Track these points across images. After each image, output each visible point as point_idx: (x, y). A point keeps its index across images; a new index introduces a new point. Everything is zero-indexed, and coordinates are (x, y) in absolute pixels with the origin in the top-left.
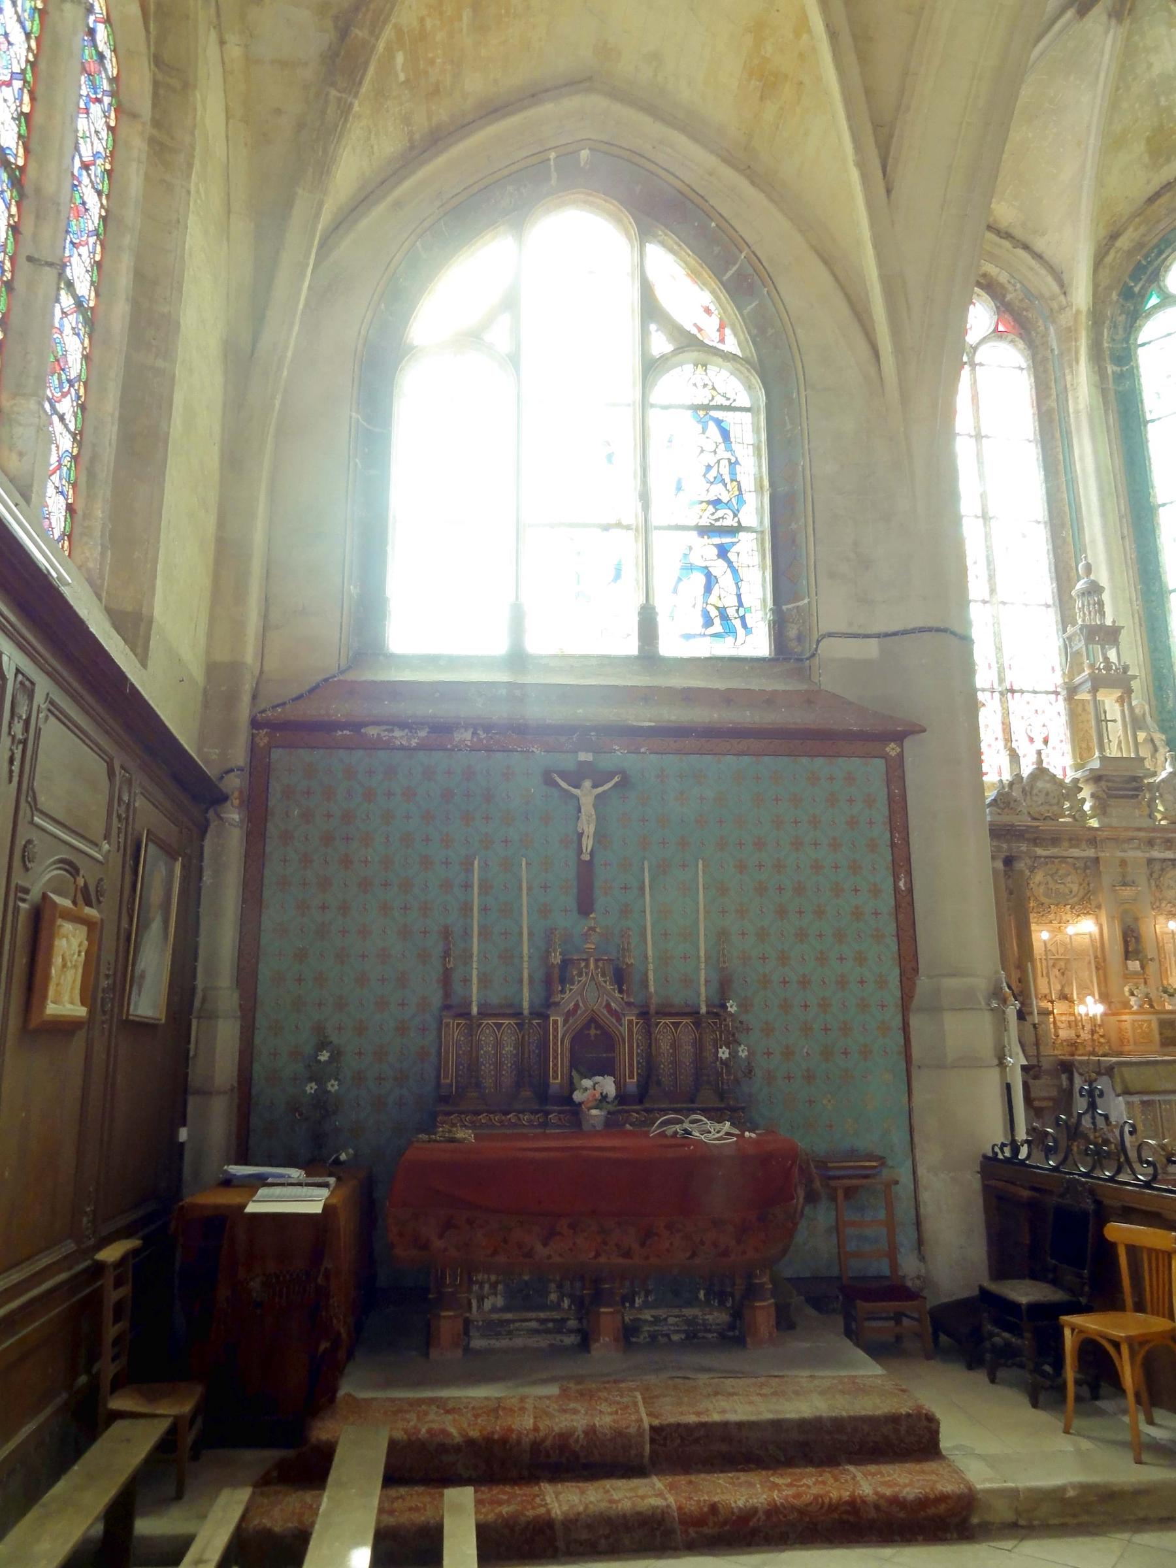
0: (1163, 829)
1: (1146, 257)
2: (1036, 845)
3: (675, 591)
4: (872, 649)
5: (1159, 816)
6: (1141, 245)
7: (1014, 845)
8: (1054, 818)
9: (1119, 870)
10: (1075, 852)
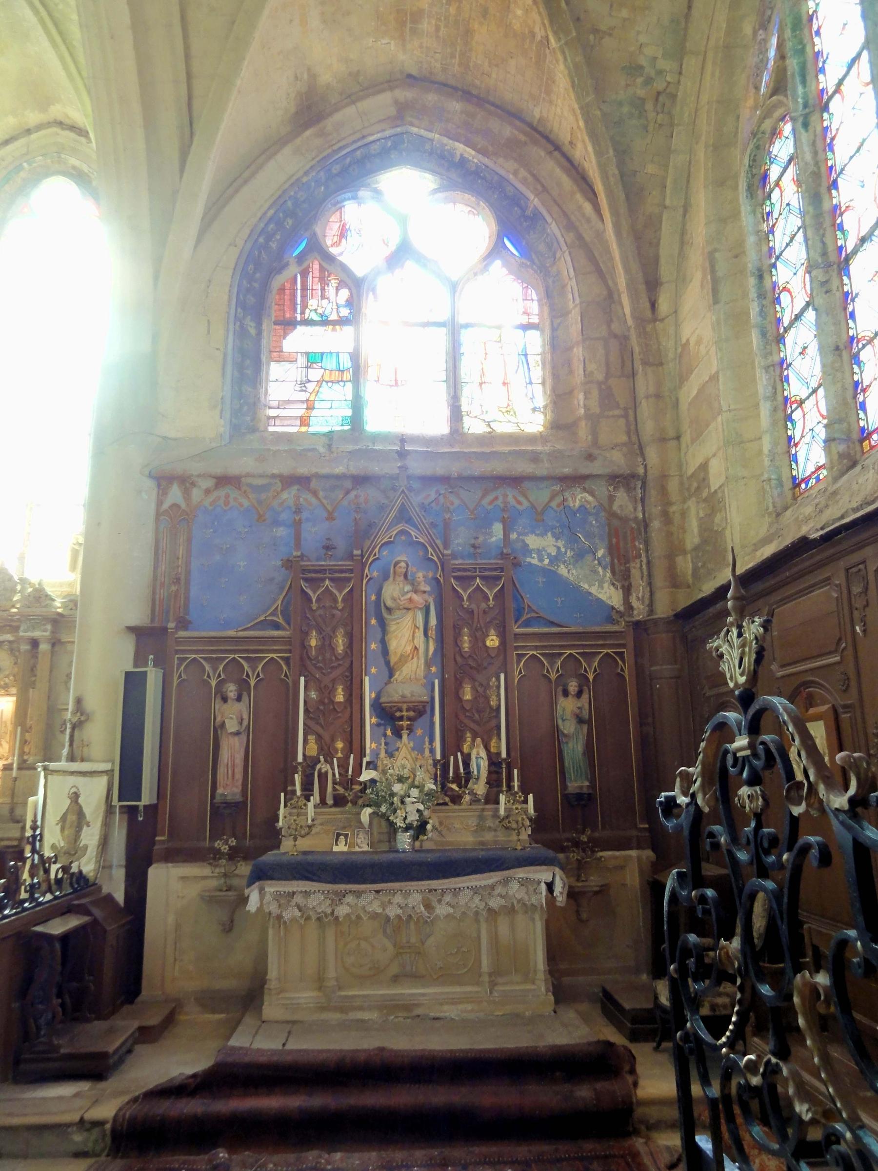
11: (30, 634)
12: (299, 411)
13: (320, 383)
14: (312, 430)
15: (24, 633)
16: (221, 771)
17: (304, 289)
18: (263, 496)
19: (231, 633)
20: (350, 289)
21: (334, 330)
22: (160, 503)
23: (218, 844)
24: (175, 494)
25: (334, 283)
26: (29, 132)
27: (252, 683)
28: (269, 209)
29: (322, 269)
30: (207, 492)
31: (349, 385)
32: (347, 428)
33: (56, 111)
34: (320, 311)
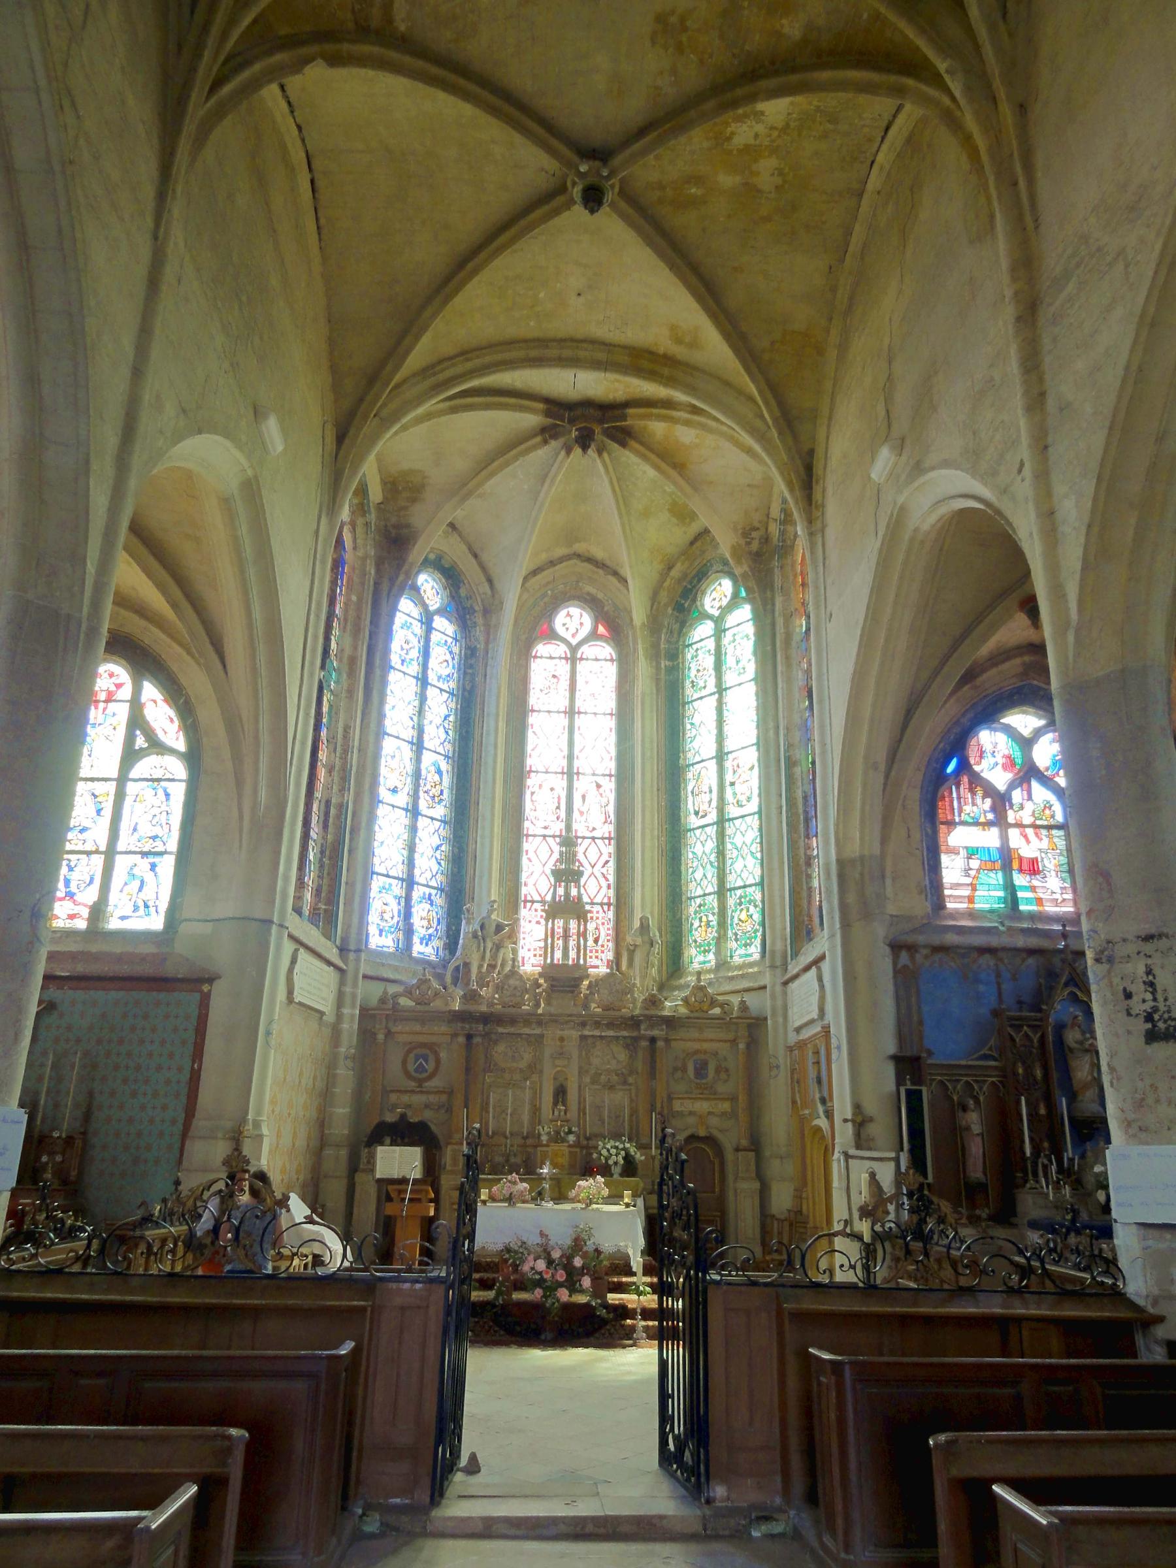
0: (595, 1015)
1: (690, 582)
2: (498, 1025)
3: (121, 891)
4: (208, 928)
5: (593, 1005)
6: (685, 575)
7: (474, 1025)
8: (518, 1005)
9: (558, 1043)
10: (527, 1031)
11: (650, 1033)
12: (966, 892)
13: (978, 871)
14: (977, 906)
15: (644, 1031)
16: (970, 1162)
17: (959, 798)
18: (966, 961)
19: (963, 1062)
20: (992, 798)
21: (984, 830)
22: (895, 964)
23: (978, 1212)
24: (904, 958)
25: (980, 793)
26: (552, 563)
27: (981, 1099)
28: (940, 742)
29: (970, 783)
30: (926, 957)
31: (1000, 874)
32: (1003, 906)
33: (579, 547)
34: (972, 815)
